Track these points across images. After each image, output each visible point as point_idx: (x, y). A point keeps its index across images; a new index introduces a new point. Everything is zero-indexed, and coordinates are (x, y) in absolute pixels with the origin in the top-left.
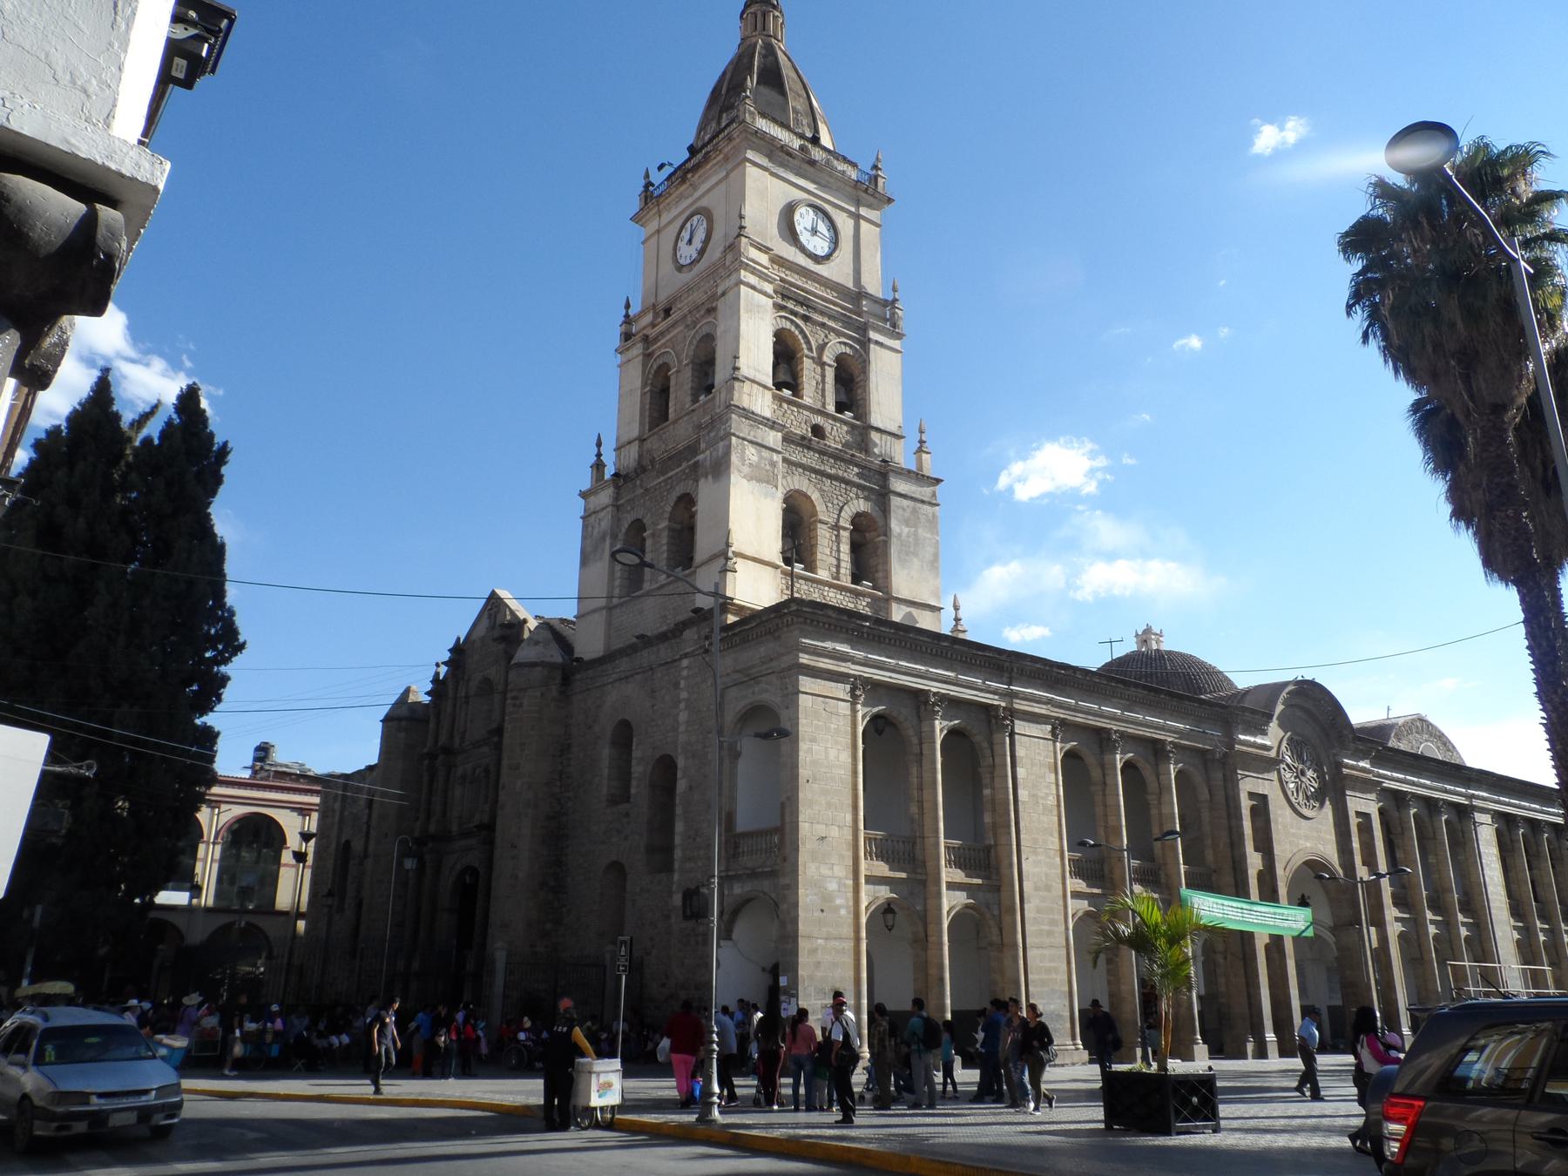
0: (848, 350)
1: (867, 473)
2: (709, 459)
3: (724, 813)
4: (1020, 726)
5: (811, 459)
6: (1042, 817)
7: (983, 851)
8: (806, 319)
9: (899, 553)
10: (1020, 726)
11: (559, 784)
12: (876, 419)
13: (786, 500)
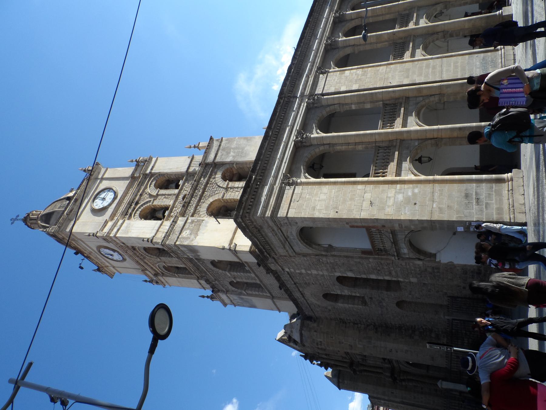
0: (154, 183)
1: (205, 173)
2: (190, 254)
3: (362, 256)
4: (319, 91)
5: (194, 201)
6: (368, 76)
7: (386, 107)
8: (137, 203)
9: (241, 157)
10: (319, 91)
11: (360, 325)
12: (184, 169)
13: (210, 216)
